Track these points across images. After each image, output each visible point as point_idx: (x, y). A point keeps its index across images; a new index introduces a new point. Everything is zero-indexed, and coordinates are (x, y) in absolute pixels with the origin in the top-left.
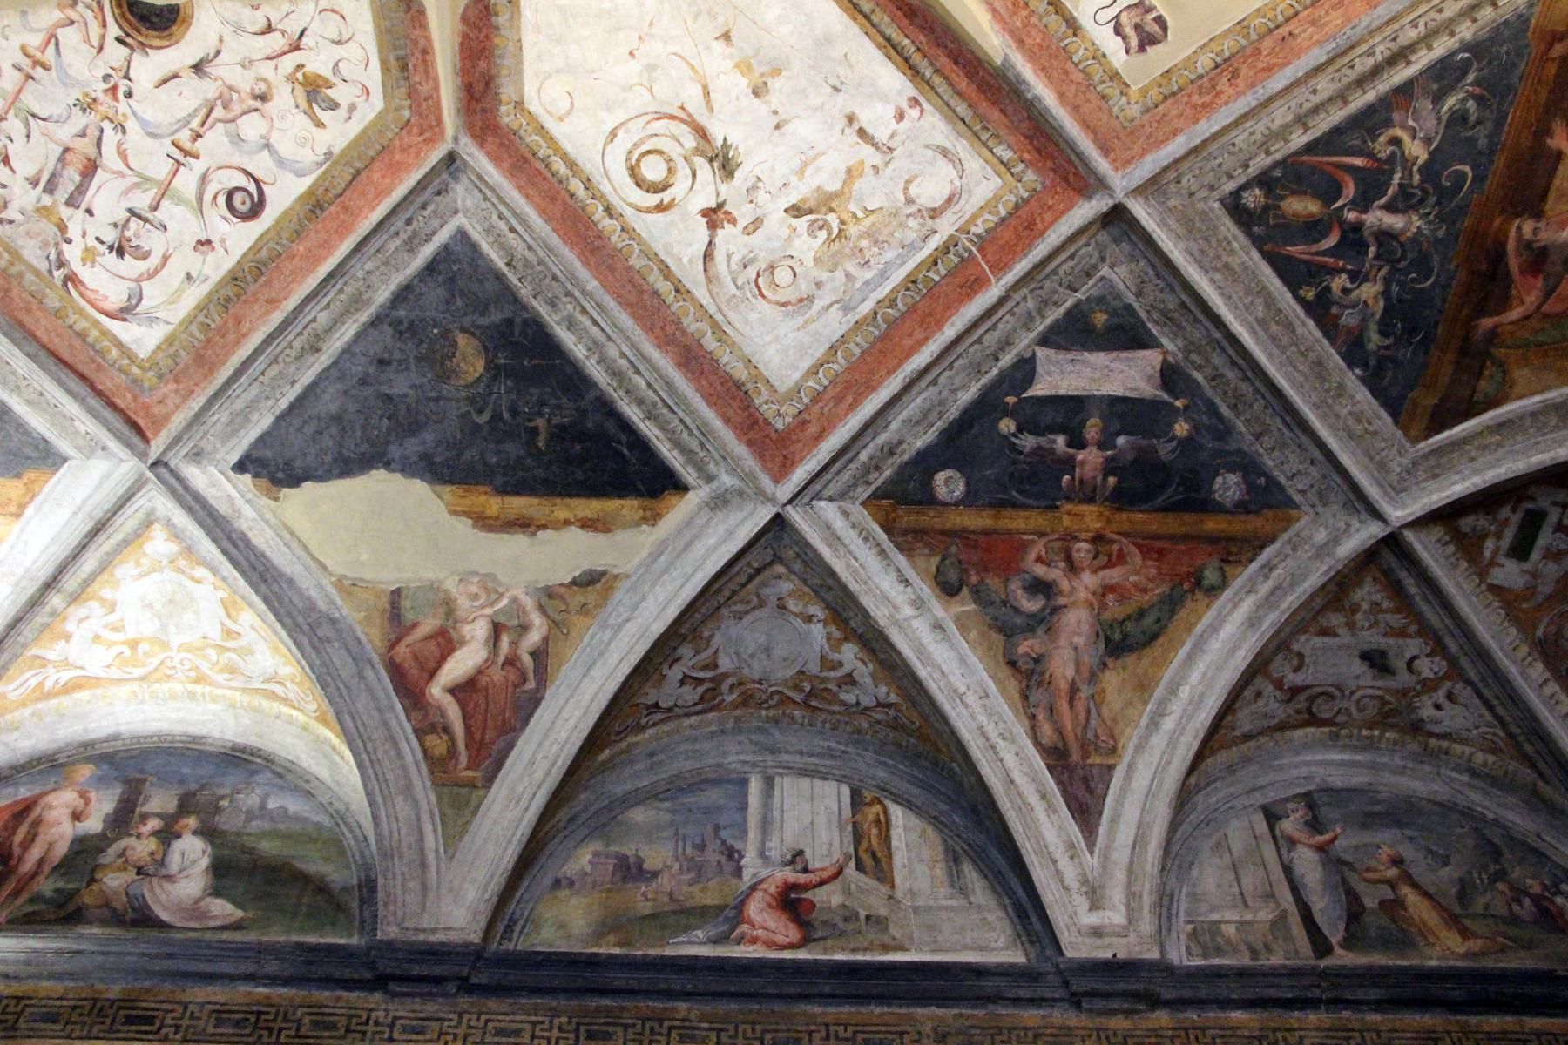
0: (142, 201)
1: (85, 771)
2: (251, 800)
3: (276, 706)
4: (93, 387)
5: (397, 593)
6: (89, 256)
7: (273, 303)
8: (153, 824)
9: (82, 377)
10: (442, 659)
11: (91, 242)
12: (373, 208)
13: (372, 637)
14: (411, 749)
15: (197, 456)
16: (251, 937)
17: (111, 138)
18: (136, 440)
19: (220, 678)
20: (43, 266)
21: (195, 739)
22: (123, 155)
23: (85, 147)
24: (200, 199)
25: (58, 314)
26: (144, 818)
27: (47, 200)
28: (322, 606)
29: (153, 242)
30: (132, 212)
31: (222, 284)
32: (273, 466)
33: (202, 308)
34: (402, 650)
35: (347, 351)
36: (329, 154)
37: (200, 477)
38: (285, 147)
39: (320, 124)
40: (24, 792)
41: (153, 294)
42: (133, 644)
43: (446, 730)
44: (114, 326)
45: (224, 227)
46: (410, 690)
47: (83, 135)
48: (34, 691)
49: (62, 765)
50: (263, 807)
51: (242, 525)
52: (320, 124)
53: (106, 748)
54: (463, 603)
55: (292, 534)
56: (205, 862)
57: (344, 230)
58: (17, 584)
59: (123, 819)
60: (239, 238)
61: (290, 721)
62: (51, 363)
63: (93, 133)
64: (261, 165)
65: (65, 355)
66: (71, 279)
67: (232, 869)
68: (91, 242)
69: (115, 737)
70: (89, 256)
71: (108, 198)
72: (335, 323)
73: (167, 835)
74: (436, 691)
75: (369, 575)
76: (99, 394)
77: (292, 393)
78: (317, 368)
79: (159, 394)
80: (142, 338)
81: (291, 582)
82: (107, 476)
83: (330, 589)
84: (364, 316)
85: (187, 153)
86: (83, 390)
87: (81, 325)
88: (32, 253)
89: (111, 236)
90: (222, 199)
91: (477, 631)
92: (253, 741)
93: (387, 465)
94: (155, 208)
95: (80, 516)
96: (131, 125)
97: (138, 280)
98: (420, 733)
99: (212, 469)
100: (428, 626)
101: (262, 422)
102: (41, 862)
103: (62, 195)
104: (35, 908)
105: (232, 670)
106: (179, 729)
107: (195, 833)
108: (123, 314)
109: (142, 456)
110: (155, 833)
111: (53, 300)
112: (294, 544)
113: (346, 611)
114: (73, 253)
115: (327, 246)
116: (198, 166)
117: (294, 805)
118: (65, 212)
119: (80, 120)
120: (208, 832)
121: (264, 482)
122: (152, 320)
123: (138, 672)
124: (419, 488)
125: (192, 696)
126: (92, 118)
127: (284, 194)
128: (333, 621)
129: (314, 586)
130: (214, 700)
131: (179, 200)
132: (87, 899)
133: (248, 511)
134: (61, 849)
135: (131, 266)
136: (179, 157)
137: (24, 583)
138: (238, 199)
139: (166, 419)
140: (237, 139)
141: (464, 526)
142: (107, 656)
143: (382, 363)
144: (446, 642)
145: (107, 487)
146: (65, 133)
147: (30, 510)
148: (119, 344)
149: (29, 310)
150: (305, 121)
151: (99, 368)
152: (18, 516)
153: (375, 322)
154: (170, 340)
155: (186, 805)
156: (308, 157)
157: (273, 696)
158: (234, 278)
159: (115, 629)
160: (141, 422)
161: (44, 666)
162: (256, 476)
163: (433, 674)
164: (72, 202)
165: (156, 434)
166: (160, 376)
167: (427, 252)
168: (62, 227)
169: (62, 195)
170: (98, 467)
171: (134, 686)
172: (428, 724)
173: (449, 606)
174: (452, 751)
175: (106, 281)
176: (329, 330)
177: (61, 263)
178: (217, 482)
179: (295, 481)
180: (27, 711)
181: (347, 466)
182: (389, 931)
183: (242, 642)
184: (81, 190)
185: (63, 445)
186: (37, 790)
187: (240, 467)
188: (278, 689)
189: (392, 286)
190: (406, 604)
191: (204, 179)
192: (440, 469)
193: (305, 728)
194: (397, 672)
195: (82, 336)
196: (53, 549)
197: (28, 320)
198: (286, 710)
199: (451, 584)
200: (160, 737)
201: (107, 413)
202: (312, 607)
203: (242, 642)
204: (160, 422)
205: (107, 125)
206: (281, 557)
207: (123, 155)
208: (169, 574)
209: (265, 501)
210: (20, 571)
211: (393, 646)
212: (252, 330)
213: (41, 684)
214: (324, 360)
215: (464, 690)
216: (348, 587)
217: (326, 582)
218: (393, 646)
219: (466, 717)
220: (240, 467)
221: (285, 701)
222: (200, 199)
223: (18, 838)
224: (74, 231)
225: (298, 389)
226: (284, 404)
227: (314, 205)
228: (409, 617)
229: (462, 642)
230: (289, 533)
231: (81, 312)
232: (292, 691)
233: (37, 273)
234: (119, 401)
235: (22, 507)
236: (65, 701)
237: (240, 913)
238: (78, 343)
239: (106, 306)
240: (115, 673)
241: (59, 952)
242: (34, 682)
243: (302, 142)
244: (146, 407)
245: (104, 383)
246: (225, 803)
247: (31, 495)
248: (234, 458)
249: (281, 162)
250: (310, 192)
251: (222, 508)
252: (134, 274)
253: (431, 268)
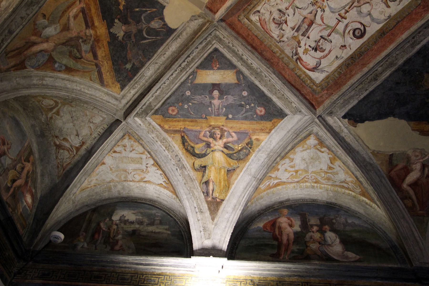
0: (325, 33)
1: (285, 211)
2: (342, 220)
3: (343, 190)
4: (300, 93)
5: (391, 156)
6: (306, 52)
7: (364, 65)
8: (315, 228)
9: (298, 90)
10: (406, 176)
11: (307, 47)
12: (402, 34)
13: (383, 169)
14: (401, 204)
15: (331, 114)
16: (365, 264)
17: (319, 13)
18: (312, 109)
19: (324, 182)
20: (290, 55)
21: (314, 200)
22: (322, 19)
23: (311, 17)
24: (344, 32)
25: (293, 70)
26: (312, 226)
27: (296, 34)
28: (368, 160)
29: (327, 46)
30: (322, 37)
31: (348, 59)
32: (355, 117)
33: (340, 67)
34: (393, 172)
35: (386, 80)
36: (389, 16)
37: (330, 120)
38: (375, 14)
39: (388, 7)
40: (270, 218)
41: (324, 63)
42: (297, 172)
43: (410, 198)
44: (310, 73)
45: (351, 41)
46: (397, 186)
47: (311, 13)
48: (267, 187)
49: (278, 209)
50: (347, 222)
51: (343, 135)
52: (388, 7)
53: (287, 204)
54: (413, 158)
55: (359, 137)
56: (338, 240)
57: (391, 41)
58: (268, 154)
59: (305, 225)
60: (355, 44)
61: (349, 195)
62: (289, 85)
63: (314, 12)
64: (366, 20)
65: (293, 83)
66: (299, 59)
67: (347, 242)
68: (307, 47)
69: (288, 200)
70: (306, 52)
71: (315, 33)
72: (383, 71)
73: (322, 232)
74: (405, 186)
75: (382, 150)
76: (302, 95)
77: (365, 94)
78: (375, 86)
79: (321, 94)
80: (318, 77)
81: (358, 152)
82: (300, 120)
83: (370, 154)
84: (393, 69)
85: (342, 18)
86: (298, 94)
87: (299, 73)
88: (288, 51)
89: (313, 45)
90: (351, 32)
91: (418, 166)
92: (333, 201)
93: (394, 116)
94: (329, 35)
95: (290, 133)
96: (327, 9)
97: (320, 59)
98: (402, 199)
99: (335, 118)
100: (401, 166)
101: (354, 102)
102: (288, 240)
103: (301, 32)
104: (294, 255)
105: (329, 179)
106: (307, 197)
107: (330, 231)
108: (313, 70)
109: (315, 114)
110: (318, 231)
111: (292, 66)
112: (360, 141)
113: (374, 161)
114: (301, 51)
115: (384, 47)
116: (345, 22)
117: (357, 222)
118: (301, 37)
119: (311, 8)
120: (333, 230)
121: (352, 121)
122: (322, 71)
123: (296, 180)
124: (403, 122)
125: (313, 187)
126: (315, 7)
127: (373, 29)
128: (371, 165)
129: (366, 154)
130: (321, 188)
131: (337, 33)
132: (309, 252)
133: (345, 130)
134: (292, 236)
135: (319, 54)
136: (340, 19)
137: (271, 154)
138: (356, 33)
139: (323, 102)
140: (360, 13)
141: (416, 134)
142: (287, 175)
143: (397, 83)
144: (407, 170)
145: (300, 124)
146: (305, 13)
147: (273, 131)
148: (310, 79)
149: (284, 69)
150: (383, 5)
151: (303, 86)
152: (269, 133)
153: (396, 71)
154: (327, 77)
155: (323, 222)
156: (382, 17)
157: (343, 187)
158: (352, 57)
159: (292, 167)
160: (314, 103)
161: (271, 179)
162: (349, 119)
163: (403, 180)
164: (303, 35)
165: (318, 107)
166: (322, 89)
167: (418, 47)
168: (299, 42)
169: (301, 32)
170: (298, 117)
171: (295, 184)
172: (405, 197)
173: (408, 159)
174: (414, 204)
175: (310, 59)
176: (381, 73)
177: (297, 54)
178: (336, 122)
179: (362, 121)
180: (265, 193)
181: (380, 116)
182: (416, 264)
183: (335, 170)
184: (307, 30)
185: (287, 111)
186: (274, 218)
187: (344, 117)
188: (345, 185)
189: (405, 59)
190: (394, 158)
191: (347, 26)
192: (408, 117)
193: (354, 197)
194: (391, 179)
195: (299, 77)
196: (280, 144)
197: (283, 72)
198: (347, 191)
199: (410, 152)
200: (303, 200)
201: (304, 101)
202: (364, 160)
203: (335, 170)
204: (320, 103)
205: (319, 10)
206: (355, 145)
207: (322, 19)
208: (313, 150)
209: (351, 127)
210: (269, 150)
211: (390, 172)
212: (356, 74)
213: (269, 184)
214: (378, 83)
215: (414, 185)
216: (375, 154)
217: (369, 152)
218: (390, 172)
219: (416, 194)
220: (344, 117)
221: (348, 188)
222: (344, 32)
223: (277, 233)
224: (302, 44)
225: (368, 92)
226: (362, 97)
227: (382, 33)
228: (395, 162)
229: (412, 170)
230: (358, 138)
231: (300, 69)
232: (351, 185)
233: (288, 57)
234: (307, 97)
235: (271, 130)
236: (275, 189)
237: (358, 257)
238: (297, 79)
239: (309, 67)
240: (290, 180)
241: (315, 269)
242: (268, 184)
243: (382, 13)
244: (316, 99)
245: (304, 91)
246: (334, 221)
247: (274, 126)
248: (343, 114)
249: (373, 20)
250: (381, 29)
251: (337, 130)
252: (319, 57)
253: (419, 53)
